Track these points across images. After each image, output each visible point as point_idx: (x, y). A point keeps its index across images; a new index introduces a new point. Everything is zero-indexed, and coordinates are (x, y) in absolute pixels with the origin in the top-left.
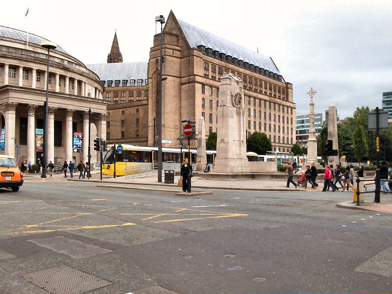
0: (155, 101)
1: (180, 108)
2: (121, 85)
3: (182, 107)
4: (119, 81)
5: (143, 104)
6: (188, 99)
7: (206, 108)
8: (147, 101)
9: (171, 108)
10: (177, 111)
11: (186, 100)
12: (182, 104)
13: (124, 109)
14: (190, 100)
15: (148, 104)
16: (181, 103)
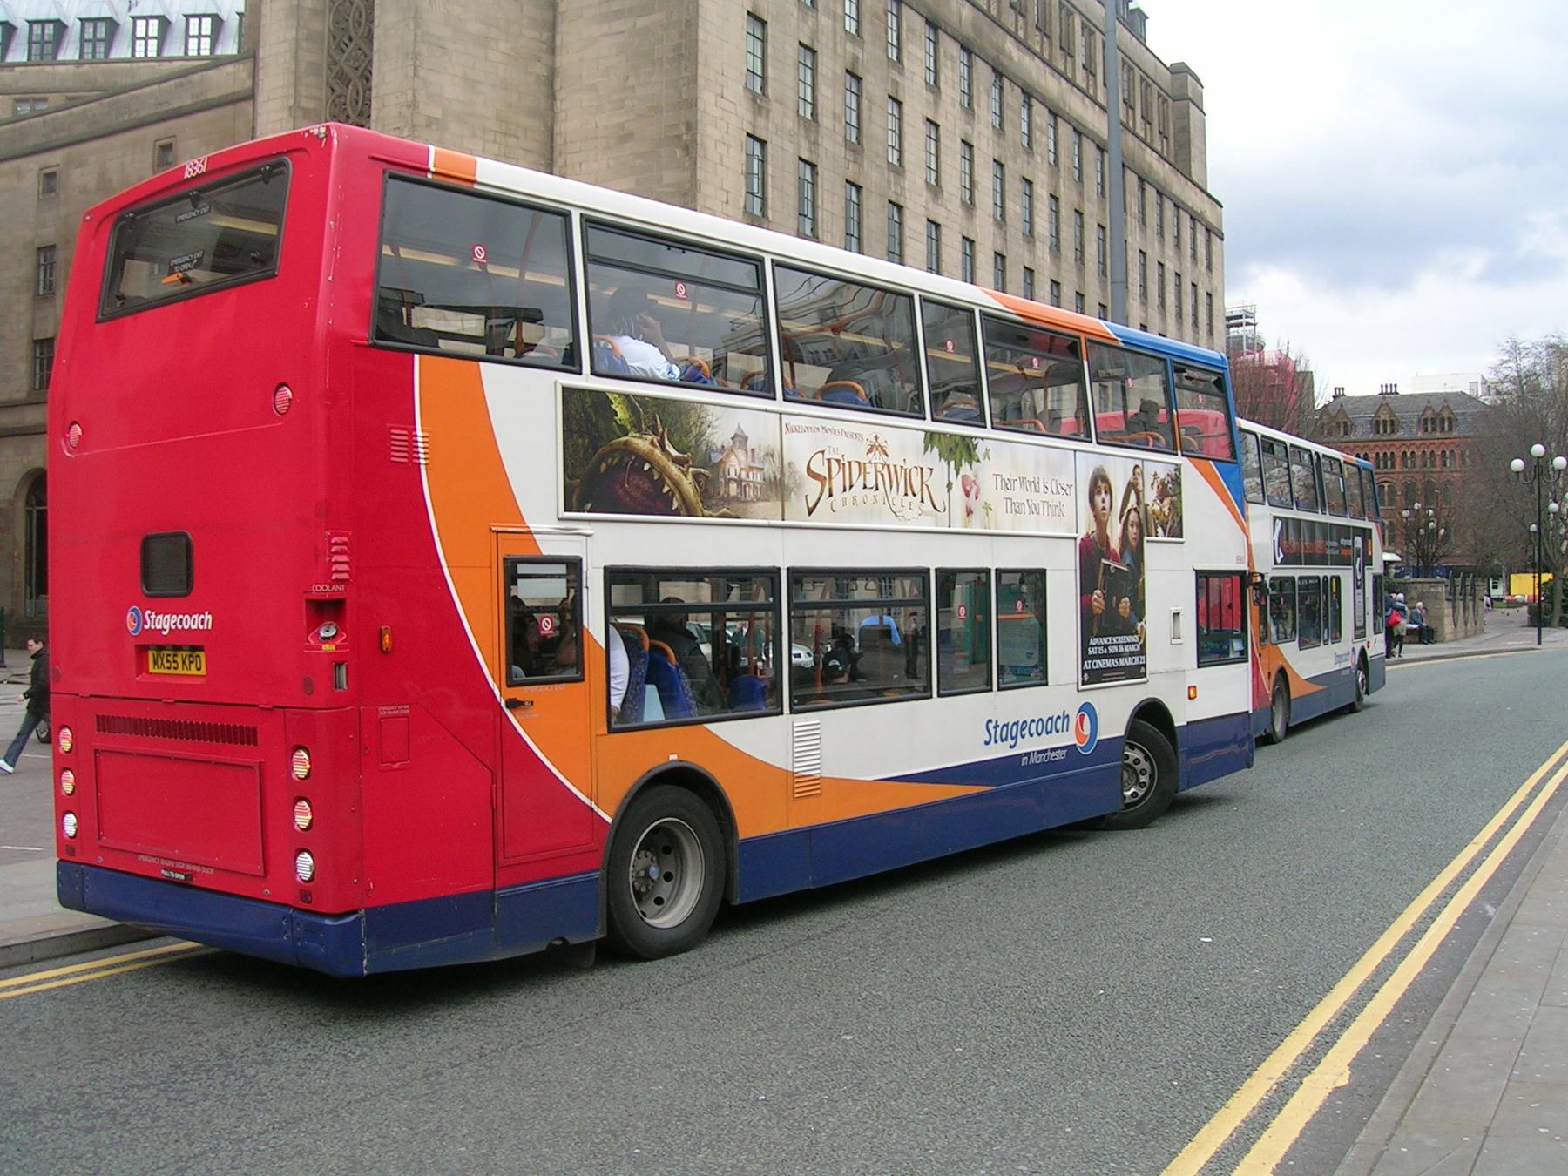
0: (322, 26)
1: (552, 97)
2: (69, 52)
3: (558, 81)
4: (60, 27)
5: (213, 94)
6: (619, 14)
7: (774, 106)
8: (241, 72)
9: (470, 83)
10: (525, 120)
11: (605, 18)
12: (565, 60)
13: (55, 158)
14: (643, 22)
15: (251, 96)
16: (552, 51)
